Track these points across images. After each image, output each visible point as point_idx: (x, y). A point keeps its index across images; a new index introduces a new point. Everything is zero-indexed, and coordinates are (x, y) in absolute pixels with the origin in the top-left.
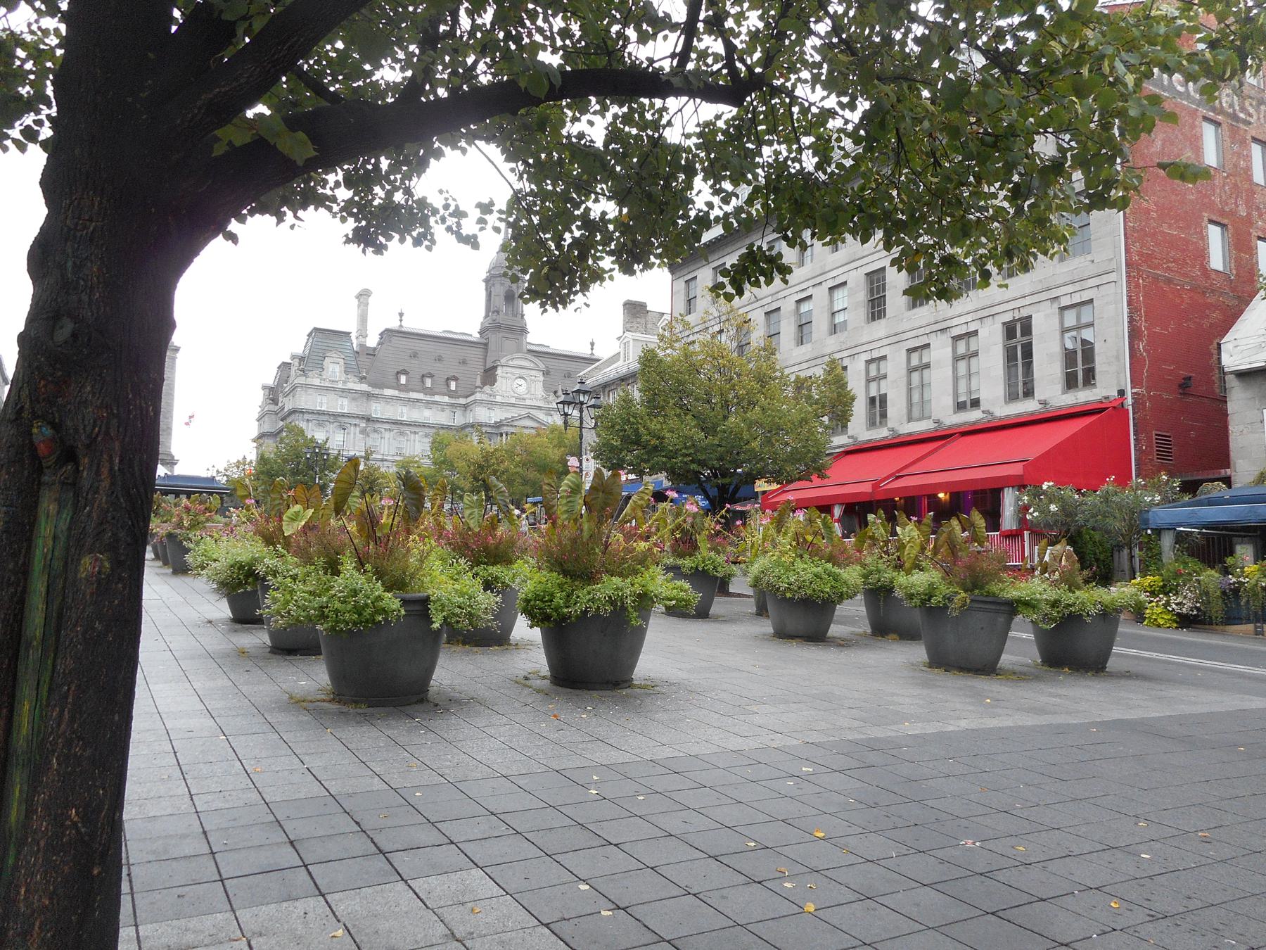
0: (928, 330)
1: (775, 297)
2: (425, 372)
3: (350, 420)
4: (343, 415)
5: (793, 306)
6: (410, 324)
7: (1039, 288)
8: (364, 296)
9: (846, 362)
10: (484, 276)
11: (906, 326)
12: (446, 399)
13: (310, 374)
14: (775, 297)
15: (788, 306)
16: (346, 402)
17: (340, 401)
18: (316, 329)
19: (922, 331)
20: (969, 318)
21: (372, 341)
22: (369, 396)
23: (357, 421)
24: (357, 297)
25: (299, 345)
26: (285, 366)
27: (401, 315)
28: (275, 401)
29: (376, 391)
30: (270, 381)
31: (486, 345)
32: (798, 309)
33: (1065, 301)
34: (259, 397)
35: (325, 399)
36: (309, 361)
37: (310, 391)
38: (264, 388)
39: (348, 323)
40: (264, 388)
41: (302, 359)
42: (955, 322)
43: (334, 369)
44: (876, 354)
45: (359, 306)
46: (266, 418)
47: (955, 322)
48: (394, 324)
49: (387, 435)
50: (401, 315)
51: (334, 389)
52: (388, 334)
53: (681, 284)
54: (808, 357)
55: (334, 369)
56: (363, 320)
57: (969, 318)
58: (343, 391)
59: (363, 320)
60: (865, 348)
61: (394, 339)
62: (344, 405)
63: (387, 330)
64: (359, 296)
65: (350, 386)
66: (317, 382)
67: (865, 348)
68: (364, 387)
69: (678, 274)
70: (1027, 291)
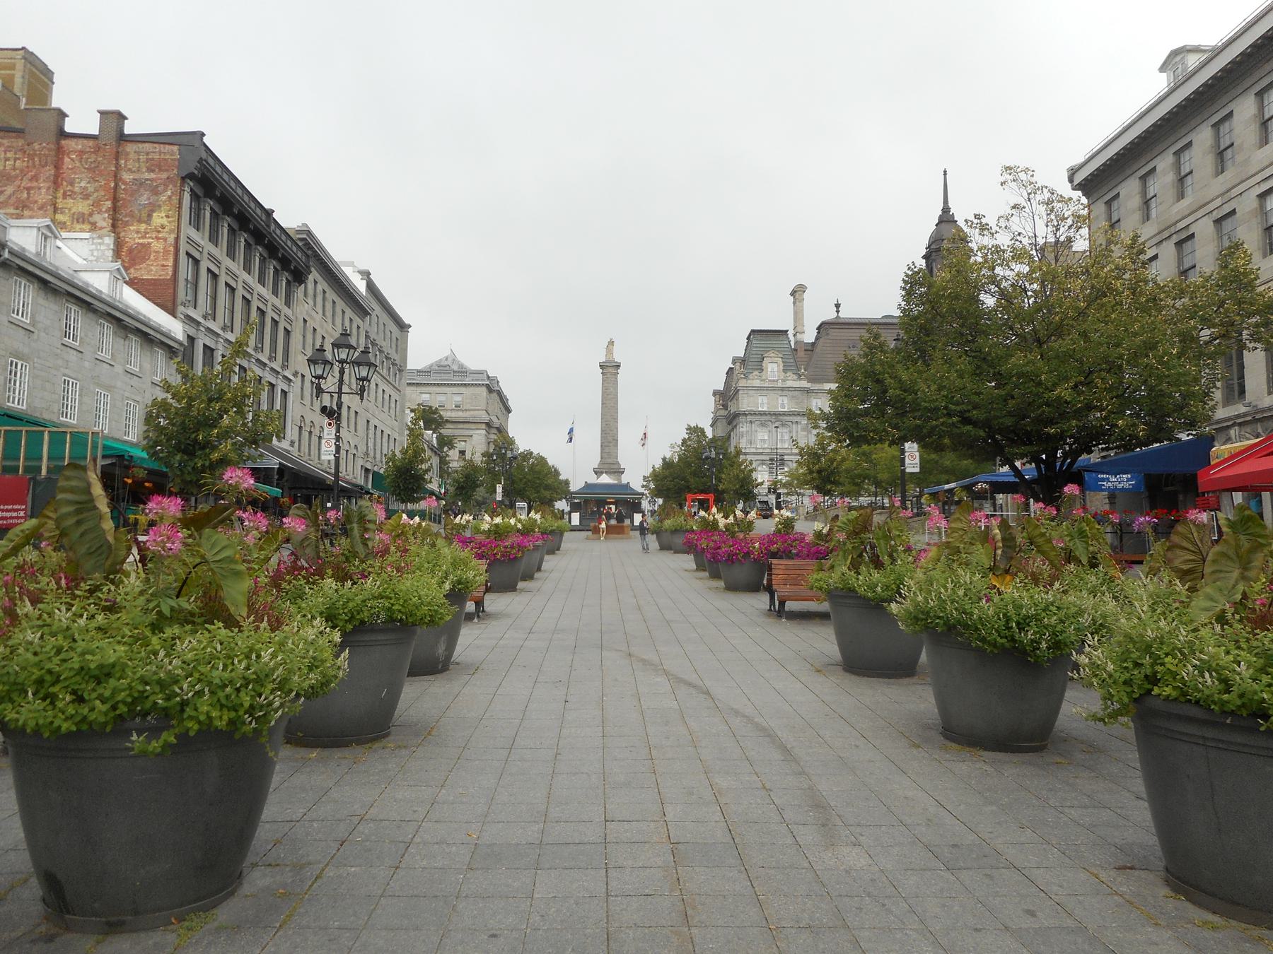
1: (1226, 197)
3: (791, 418)
4: (784, 414)
5: (1255, 204)
6: (845, 314)
8: (798, 292)
10: (924, 252)
13: (750, 376)
14: (1226, 197)
15: (1247, 204)
16: (786, 400)
17: (780, 400)
18: (753, 331)
21: (810, 336)
22: (808, 392)
26: (730, 371)
27: (838, 306)
28: (725, 407)
29: (816, 387)
32: (1262, 206)
34: (710, 404)
35: (765, 399)
36: (748, 363)
37: (751, 393)
38: (715, 393)
39: (783, 321)
40: (715, 393)
41: (743, 361)
43: (773, 368)
45: (794, 303)
46: (718, 424)
48: (830, 315)
50: (838, 306)
51: (774, 389)
52: (823, 327)
53: (1100, 208)
55: (773, 368)
56: (798, 316)
58: (783, 389)
59: (798, 316)
61: (834, 333)
62: (784, 404)
63: (823, 323)
64: (793, 293)
65: (789, 384)
66: (757, 383)
68: (804, 384)
69: (1096, 196)
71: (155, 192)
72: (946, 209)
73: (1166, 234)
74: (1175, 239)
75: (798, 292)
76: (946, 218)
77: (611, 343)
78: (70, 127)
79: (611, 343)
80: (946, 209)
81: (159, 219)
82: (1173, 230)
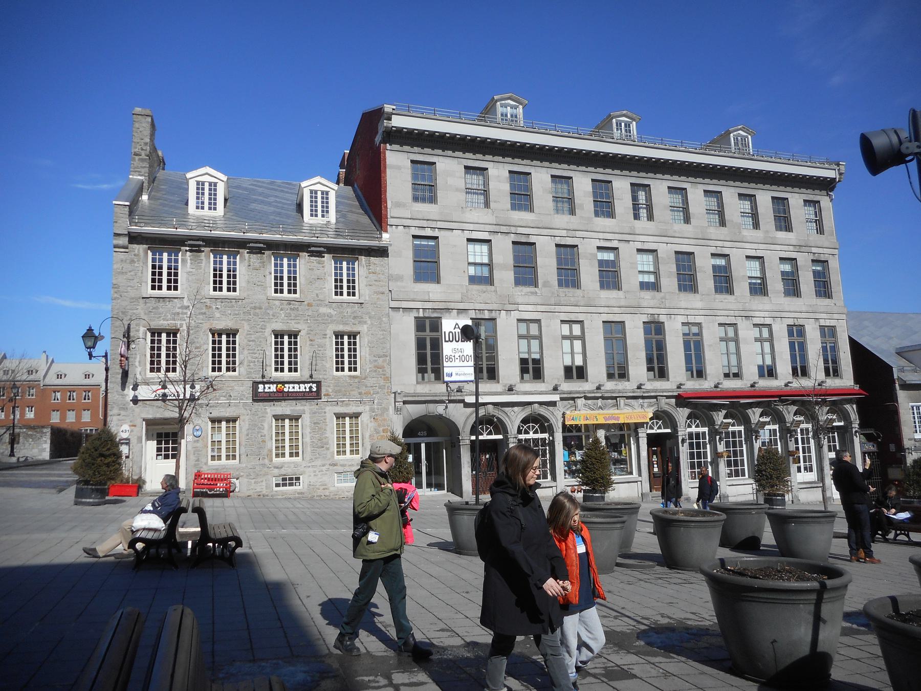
0: (737, 313)
1: (571, 233)
7: (811, 310)
9: (662, 318)
11: (720, 306)
14: (571, 233)
19: (732, 313)
20: (767, 314)
33: (823, 323)
42: (757, 314)
44: (691, 319)
47: (757, 314)
54: (623, 303)
57: (767, 314)
60: (682, 312)
67: (682, 312)
70: (804, 309)
73: (504, 229)
74: (513, 238)
82: (513, 230)
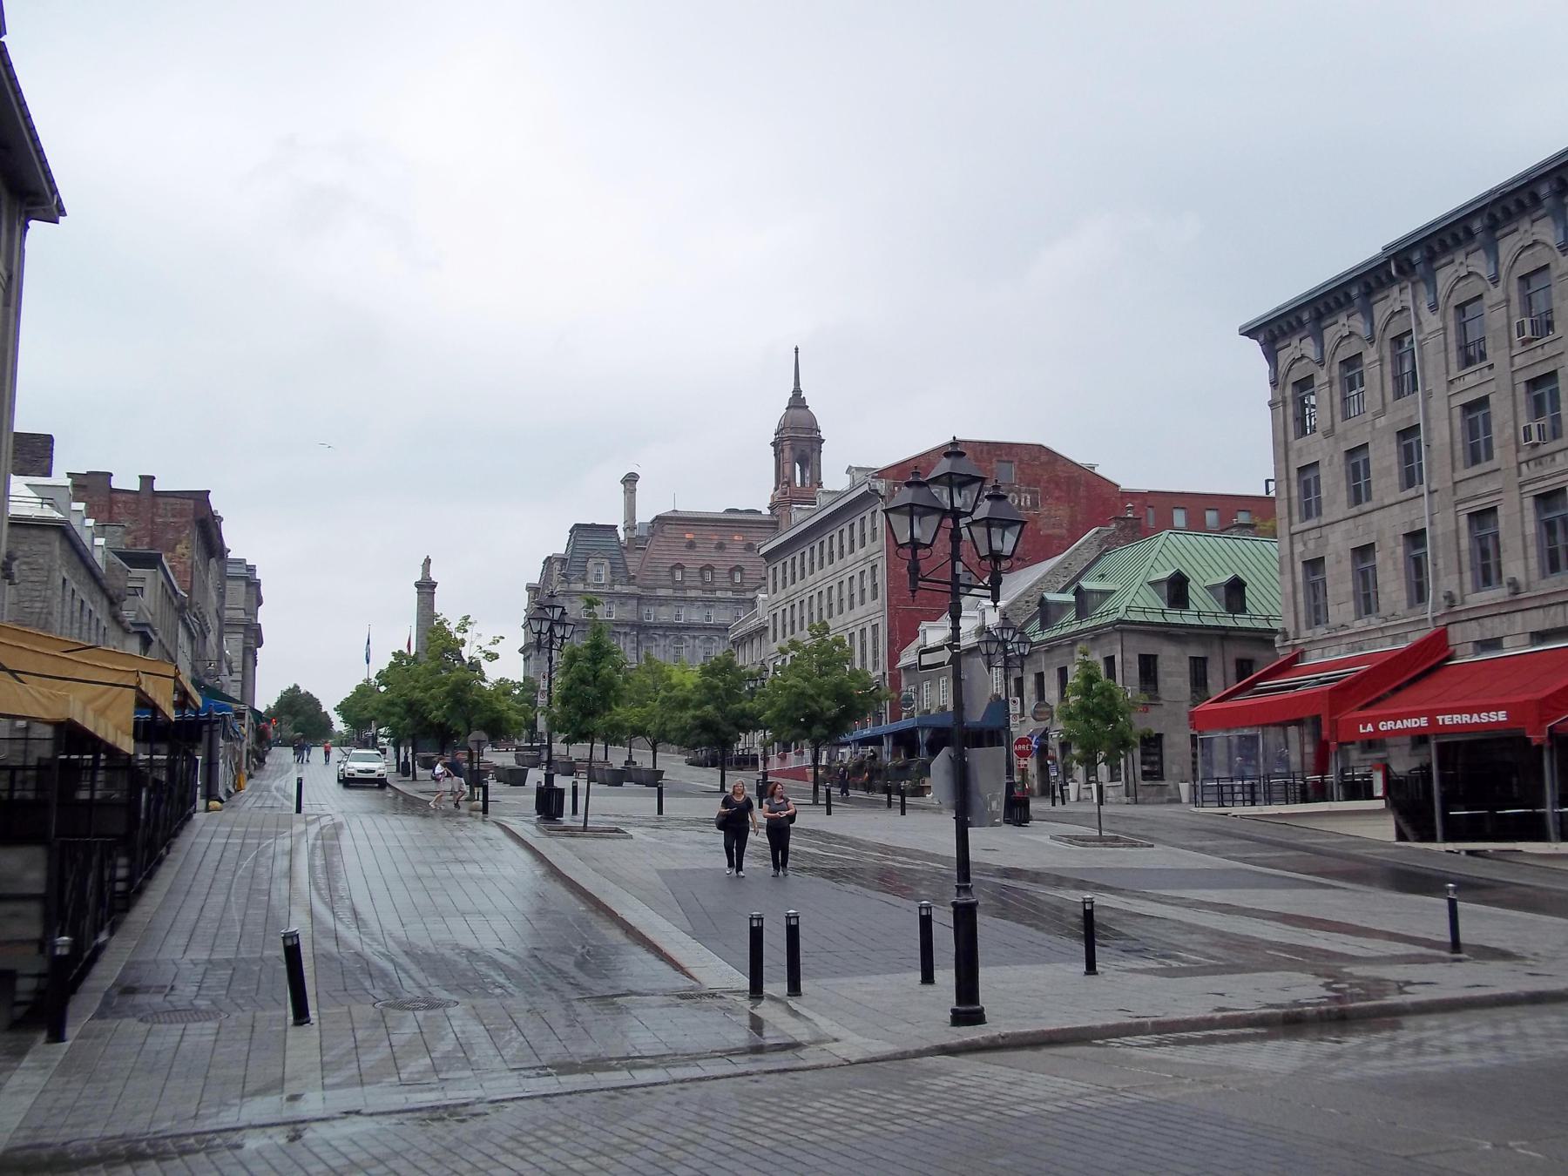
2: (702, 563)
8: (630, 480)
12: (730, 594)
18: (577, 526)
23: (627, 630)
24: (624, 481)
25: (559, 545)
30: (535, 579)
31: (776, 523)
34: (523, 599)
38: (529, 588)
39: (612, 515)
40: (529, 588)
49: (662, 643)
52: (660, 520)
64: (624, 481)
65: (617, 588)
71: (178, 530)
72: (797, 392)
75: (630, 480)
76: (797, 401)
77: (428, 561)
78: (115, 484)
79: (428, 561)
80: (797, 392)
81: (180, 549)
